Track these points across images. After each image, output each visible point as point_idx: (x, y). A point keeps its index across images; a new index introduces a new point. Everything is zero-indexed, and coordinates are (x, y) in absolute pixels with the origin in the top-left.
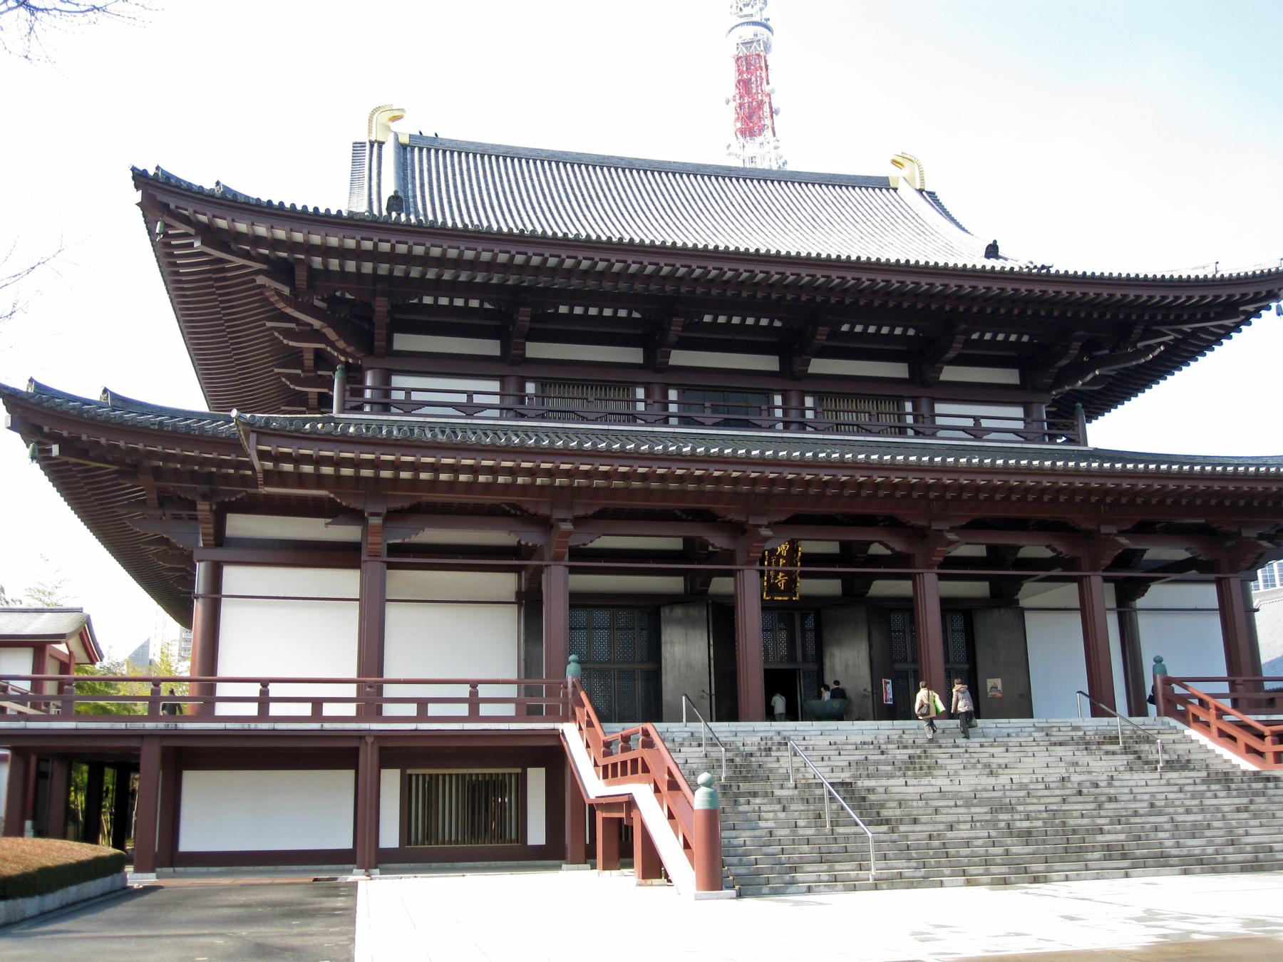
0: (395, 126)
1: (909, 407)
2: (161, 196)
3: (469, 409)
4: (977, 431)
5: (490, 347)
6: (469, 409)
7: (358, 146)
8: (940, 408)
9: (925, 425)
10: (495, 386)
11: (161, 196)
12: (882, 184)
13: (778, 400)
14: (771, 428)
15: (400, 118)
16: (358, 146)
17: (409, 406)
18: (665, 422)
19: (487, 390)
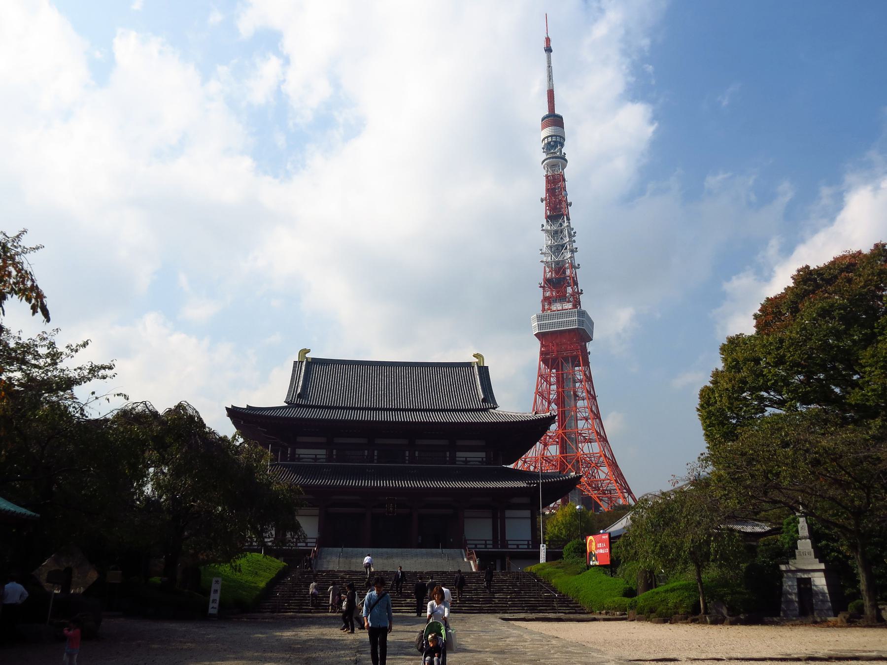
0: (307, 355)
1: (448, 454)
2: (234, 413)
3: (316, 459)
4: (466, 462)
5: (322, 440)
6: (316, 459)
7: (295, 362)
8: (459, 454)
9: (453, 460)
10: (323, 452)
11: (234, 413)
12: (469, 365)
13: (407, 453)
14: (404, 463)
15: (309, 351)
16: (295, 362)
17: (299, 459)
18: (373, 462)
19: (321, 453)
